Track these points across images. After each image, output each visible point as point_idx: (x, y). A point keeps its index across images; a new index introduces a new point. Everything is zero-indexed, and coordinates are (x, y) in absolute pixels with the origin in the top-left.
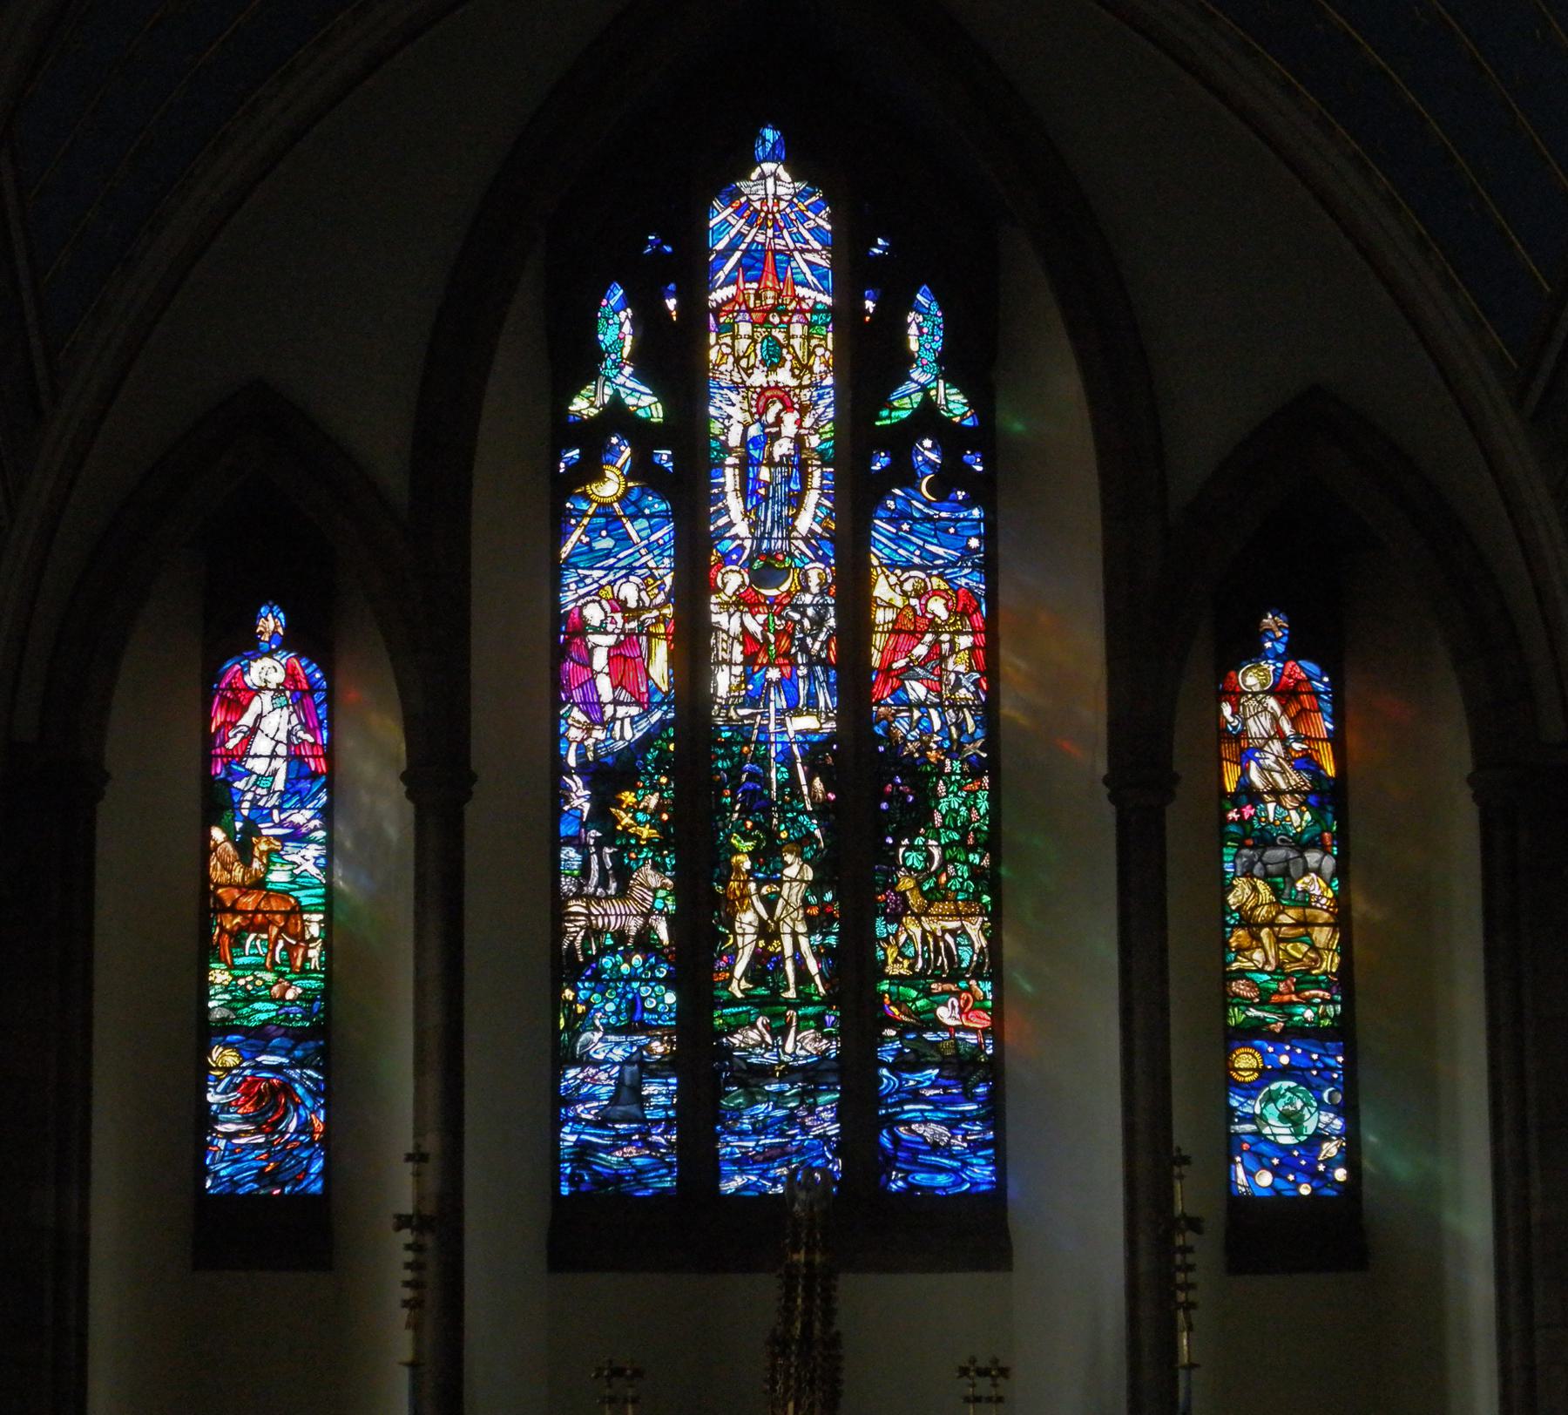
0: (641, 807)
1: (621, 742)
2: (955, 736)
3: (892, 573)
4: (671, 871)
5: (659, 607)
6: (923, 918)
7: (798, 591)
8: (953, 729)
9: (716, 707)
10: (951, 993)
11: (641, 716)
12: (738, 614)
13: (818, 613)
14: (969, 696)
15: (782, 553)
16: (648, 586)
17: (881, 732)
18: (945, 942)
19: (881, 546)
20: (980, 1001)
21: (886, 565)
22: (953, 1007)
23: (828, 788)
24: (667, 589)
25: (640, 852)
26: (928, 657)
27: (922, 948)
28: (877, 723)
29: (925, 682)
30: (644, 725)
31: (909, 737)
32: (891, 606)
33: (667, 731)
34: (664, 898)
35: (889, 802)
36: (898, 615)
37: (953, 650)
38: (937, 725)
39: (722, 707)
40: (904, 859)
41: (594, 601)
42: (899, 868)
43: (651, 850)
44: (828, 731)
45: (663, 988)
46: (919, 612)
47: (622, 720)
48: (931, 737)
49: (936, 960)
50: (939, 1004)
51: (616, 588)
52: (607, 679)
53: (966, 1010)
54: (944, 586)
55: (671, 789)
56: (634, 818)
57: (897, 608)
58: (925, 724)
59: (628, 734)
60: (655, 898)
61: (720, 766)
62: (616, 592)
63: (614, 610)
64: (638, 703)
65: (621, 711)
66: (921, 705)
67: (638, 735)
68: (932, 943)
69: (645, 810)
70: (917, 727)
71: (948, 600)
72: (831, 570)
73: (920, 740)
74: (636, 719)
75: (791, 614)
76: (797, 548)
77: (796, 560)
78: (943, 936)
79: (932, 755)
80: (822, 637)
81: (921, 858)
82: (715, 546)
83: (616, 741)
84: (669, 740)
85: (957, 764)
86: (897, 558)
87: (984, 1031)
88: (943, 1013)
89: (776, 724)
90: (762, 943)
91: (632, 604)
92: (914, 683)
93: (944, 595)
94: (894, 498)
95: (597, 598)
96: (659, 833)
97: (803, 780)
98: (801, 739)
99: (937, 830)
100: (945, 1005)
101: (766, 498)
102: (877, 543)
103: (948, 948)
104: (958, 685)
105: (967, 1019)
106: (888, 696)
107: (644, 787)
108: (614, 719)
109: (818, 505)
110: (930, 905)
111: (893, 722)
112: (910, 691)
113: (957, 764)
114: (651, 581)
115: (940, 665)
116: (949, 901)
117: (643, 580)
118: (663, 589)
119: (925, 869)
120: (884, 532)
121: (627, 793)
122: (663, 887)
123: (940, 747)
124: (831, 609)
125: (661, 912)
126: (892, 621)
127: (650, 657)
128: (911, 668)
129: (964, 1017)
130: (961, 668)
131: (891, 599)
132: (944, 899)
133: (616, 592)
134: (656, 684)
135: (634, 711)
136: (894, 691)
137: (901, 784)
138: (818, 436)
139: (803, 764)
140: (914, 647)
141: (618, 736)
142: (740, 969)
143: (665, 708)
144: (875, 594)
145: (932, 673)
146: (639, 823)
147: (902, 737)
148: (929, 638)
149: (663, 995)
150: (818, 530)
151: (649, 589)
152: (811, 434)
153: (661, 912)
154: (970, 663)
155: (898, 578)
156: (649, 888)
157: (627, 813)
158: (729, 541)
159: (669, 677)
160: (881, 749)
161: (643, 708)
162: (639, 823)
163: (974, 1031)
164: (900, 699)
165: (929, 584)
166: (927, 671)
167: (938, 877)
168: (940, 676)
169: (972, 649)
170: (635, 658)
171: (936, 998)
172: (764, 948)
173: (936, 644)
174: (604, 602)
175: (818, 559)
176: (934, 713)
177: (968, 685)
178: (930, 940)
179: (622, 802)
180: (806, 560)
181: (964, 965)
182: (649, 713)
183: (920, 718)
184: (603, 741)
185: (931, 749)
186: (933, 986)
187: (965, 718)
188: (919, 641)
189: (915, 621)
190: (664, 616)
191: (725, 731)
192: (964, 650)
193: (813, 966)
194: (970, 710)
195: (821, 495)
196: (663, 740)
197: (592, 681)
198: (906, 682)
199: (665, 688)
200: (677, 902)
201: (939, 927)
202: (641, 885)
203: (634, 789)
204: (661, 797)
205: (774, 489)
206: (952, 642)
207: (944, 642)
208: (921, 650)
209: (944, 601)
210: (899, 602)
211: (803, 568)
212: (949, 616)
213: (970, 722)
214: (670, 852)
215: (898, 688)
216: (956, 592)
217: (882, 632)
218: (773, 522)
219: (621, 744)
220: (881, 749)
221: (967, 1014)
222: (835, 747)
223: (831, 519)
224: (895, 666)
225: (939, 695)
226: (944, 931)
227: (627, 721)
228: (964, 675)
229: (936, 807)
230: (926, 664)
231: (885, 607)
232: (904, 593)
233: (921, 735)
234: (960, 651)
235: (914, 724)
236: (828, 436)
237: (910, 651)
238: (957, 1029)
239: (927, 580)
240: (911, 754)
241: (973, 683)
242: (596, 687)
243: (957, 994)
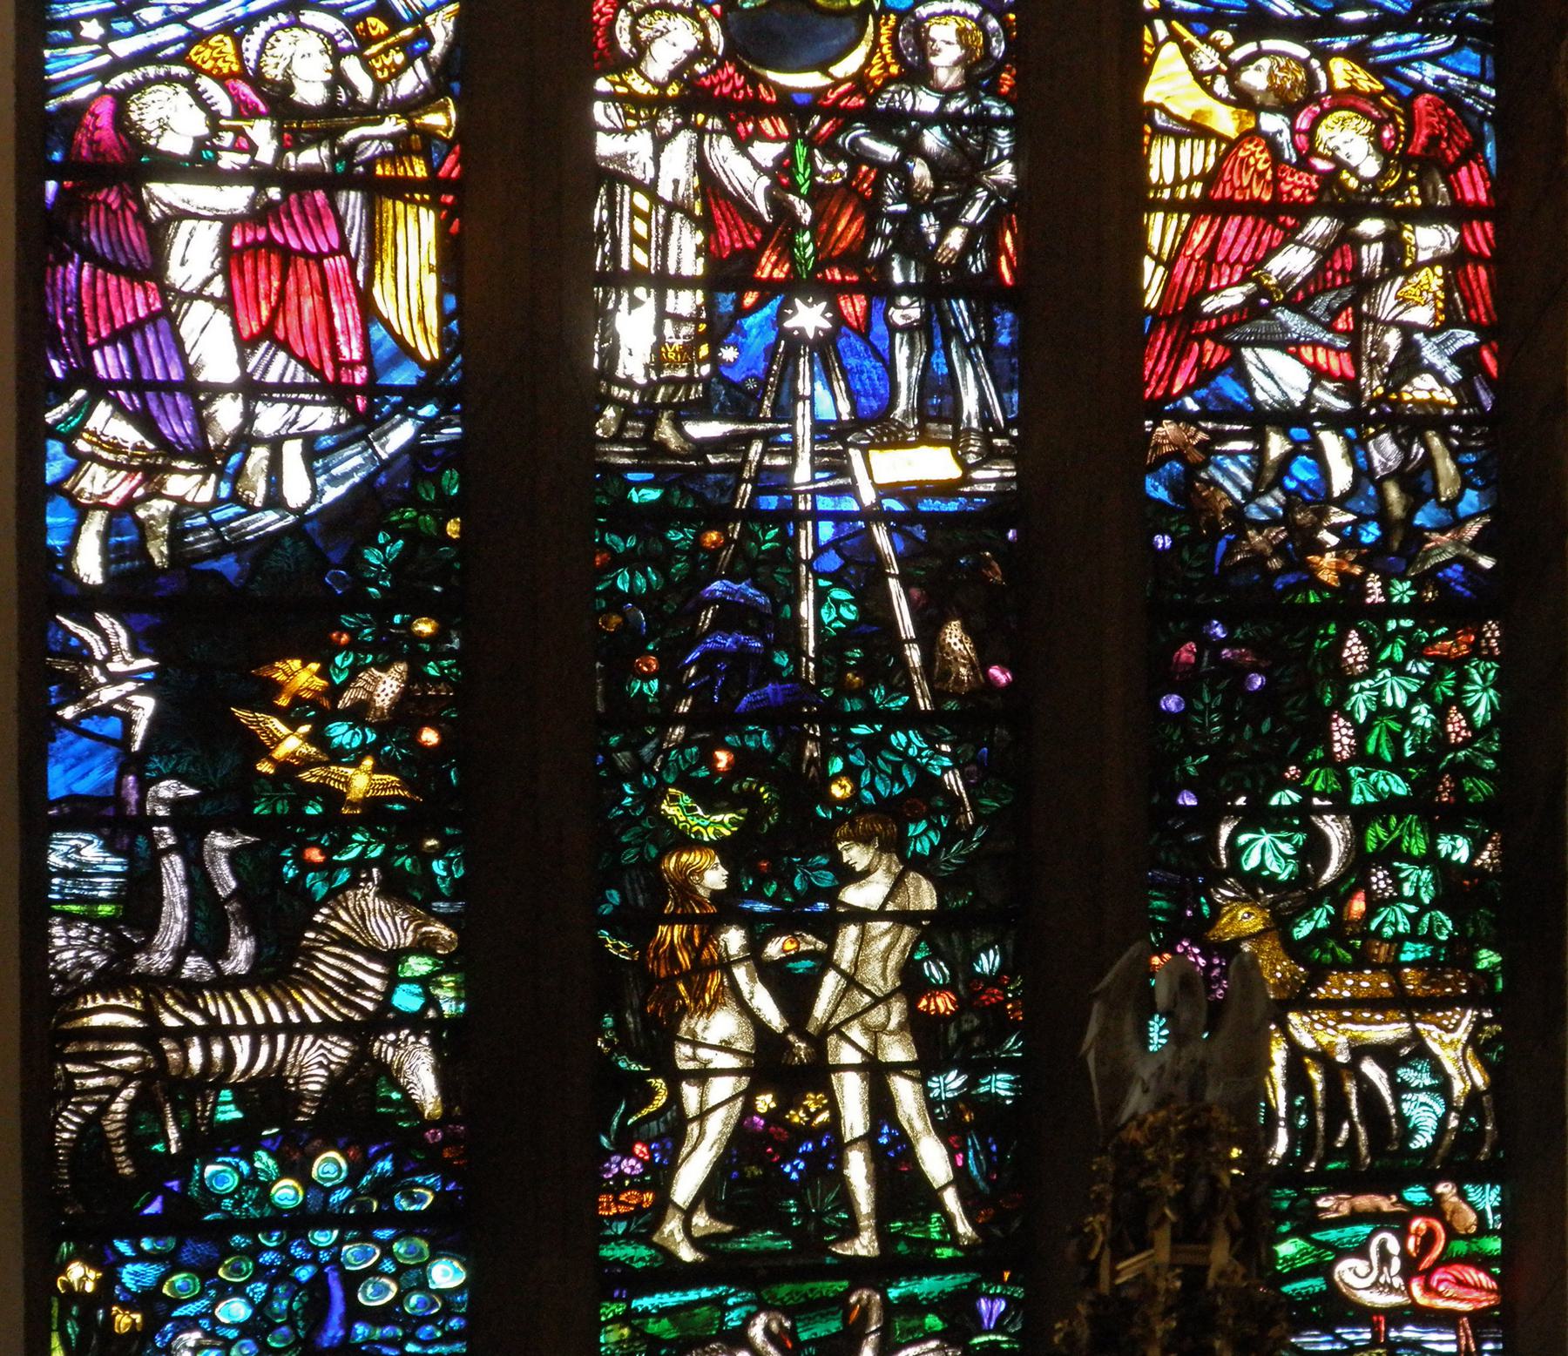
0: (346, 701)
1: (271, 516)
2: (1397, 510)
3: (1204, 39)
4: (451, 899)
5: (406, 107)
6: (1294, 1017)
8: (1393, 493)
9: (610, 413)
10: (1379, 1220)
11: (346, 436)
12: (685, 138)
14: (1445, 395)
16: (366, 40)
17: (1162, 494)
18: (1362, 1080)
20: (1467, 1237)
22: (1385, 1258)
23: (985, 652)
24: (437, 51)
25: (342, 843)
26: (1317, 282)
27: (1290, 1098)
28: (1153, 469)
29: (1307, 353)
30: (358, 460)
31: (1253, 512)
32: (1197, 130)
33: (436, 479)
34: (425, 981)
35: (1188, 693)
36: (1220, 160)
37: (1397, 261)
38: (1342, 478)
39: (628, 411)
40: (1235, 852)
41: (170, 79)
42: (1217, 878)
43: (380, 838)
44: (992, 487)
45: (423, 1245)
46: (1289, 154)
47: (275, 444)
48: (1322, 514)
49: (1332, 1130)
50: (1341, 1253)
51: (252, 45)
52: (222, 320)
53: (1426, 1264)
54: (1365, 82)
55: (450, 654)
56: (318, 738)
57: (1221, 138)
58: (1304, 476)
59: (296, 489)
60: (393, 980)
61: (623, 585)
62: (251, 55)
63: (244, 110)
64: (337, 393)
65: (270, 418)
66: (1287, 417)
67: (332, 494)
68: (1319, 1087)
69: (358, 714)
70: (1277, 483)
71: (1380, 124)
72: (1003, 22)
73: (1286, 521)
74: (326, 442)
75: (867, 142)
78: (1353, 1066)
79: (1327, 567)
80: (973, 214)
81: (1287, 849)
83: (252, 510)
84: (447, 506)
85: (1402, 591)
87: (1479, 1319)
88: (1352, 1275)
89: (815, 469)
90: (765, 1102)
91: (311, 93)
92: (1272, 357)
93: (1368, 107)
95: (183, 71)
96: (406, 783)
97: (906, 624)
98: (896, 505)
99: (1340, 769)
100: (1361, 1251)
103: (1368, 1093)
104: (1409, 363)
105: (1428, 1289)
106: (1188, 390)
107: (355, 646)
108: (244, 439)
110: (1318, 975)
111: (1204, 465)
112: (1251, 369)
113: (1402, 591)
114: (378, 26)
115: (1355, 302)
116: (1376, 968)
117: (351, 21)
118: (424, 54)
119: (1303, 879)
121: (296, 664)
122: (423, 947)
123: (1349, 541)
124: (1002, 133)
125: (415, 1022)
127: (373, 256)
128: (1265, 313)
129: (1416, 1288)
130: (1422, 315)
131: (1198, 114)
132: (1361, 961)
133: (251, 55)
134: (399, 339)
135: (320, 417)
136: (1205, 376)
137: (1228, 642)
139: (906, 582)
140: (1272, 252)
141: (258, 497)
142: (688, 1181)
143: (429, 410)
145: (1329, 327)
146: (336, 755)
147: (1227, 511)
148: (1320, 227)
149: (423, 1267)
151: (374, 49)
153: (415, 1022)
154: (1449, 300)
155: (1224, 54)
156: (373, 953)
157: (293, 725)
159: (444, 318)
160: (1162, 541)
161: (352, 408)
162: (336, 755)
163: (1446, 1319)
164: (1223, 399)
165: (1321, 76)
166: (1314, 320)
167: (1341, 903)
168: (1355, 336)
169: (1454, 262)
170: (319, 257)
171: (1332, 1235)
172: (770, 1116)
173: (1347, 240)
174: (205, 83)
176: (1332, 444)
177: (1441, 362)
178: (1316, 1075)
179: (278, 687)
181: (1421, 1141)
182: (372, 425)
183: (1287, 460)
184: (205, 509)
185: (1321, 549)
186: (1321, 1203)
187: (1429, 459)
188: (1290, 237)
189: (1276, 180)
190: (428, 134)
191: (639, 485)
192: (1431, 263)
193: (934, 1160)
194: (1445, 436)
196: (421, 506)
197: (166, 317)
198: (1247, 353)
199: (429, 349)
200: (465, 991)
201: (1342, 1040)
202: (345, 942)
203: (318, 651)
204: (415, 676)
206: (1394, 244)
207: (1370, 241)
208: (1295, 262)
209: (1367, 126)
210: (1226, 121)
212: (1385, 168)
213: (1446, 467)
214: (447, 844)
215: (1221, 368)
216: (1407, 103)
217: (1173, 206)
219: (270, 520)
220: (1162, 541)
221: (1429, 1273)
222: (1011, 534)
224: (1210, 305)
225: (1350, 389)
226: (1360, 1051)
227: (292, 451)
228: (1429, 333)
229: (1339, 705)
230: (1310, 299)
231: (1179, 137)
232: (1243, 100)
233: (1288, 507)
234: (1417, 267)
235: (1269, 475)
237: (1260, 263)
238: (1396, 1316)
239: (1315, 63)
240: (1258, 559)
241: (1455, 359)
242: (179, 342)
243: (1398, 1223)
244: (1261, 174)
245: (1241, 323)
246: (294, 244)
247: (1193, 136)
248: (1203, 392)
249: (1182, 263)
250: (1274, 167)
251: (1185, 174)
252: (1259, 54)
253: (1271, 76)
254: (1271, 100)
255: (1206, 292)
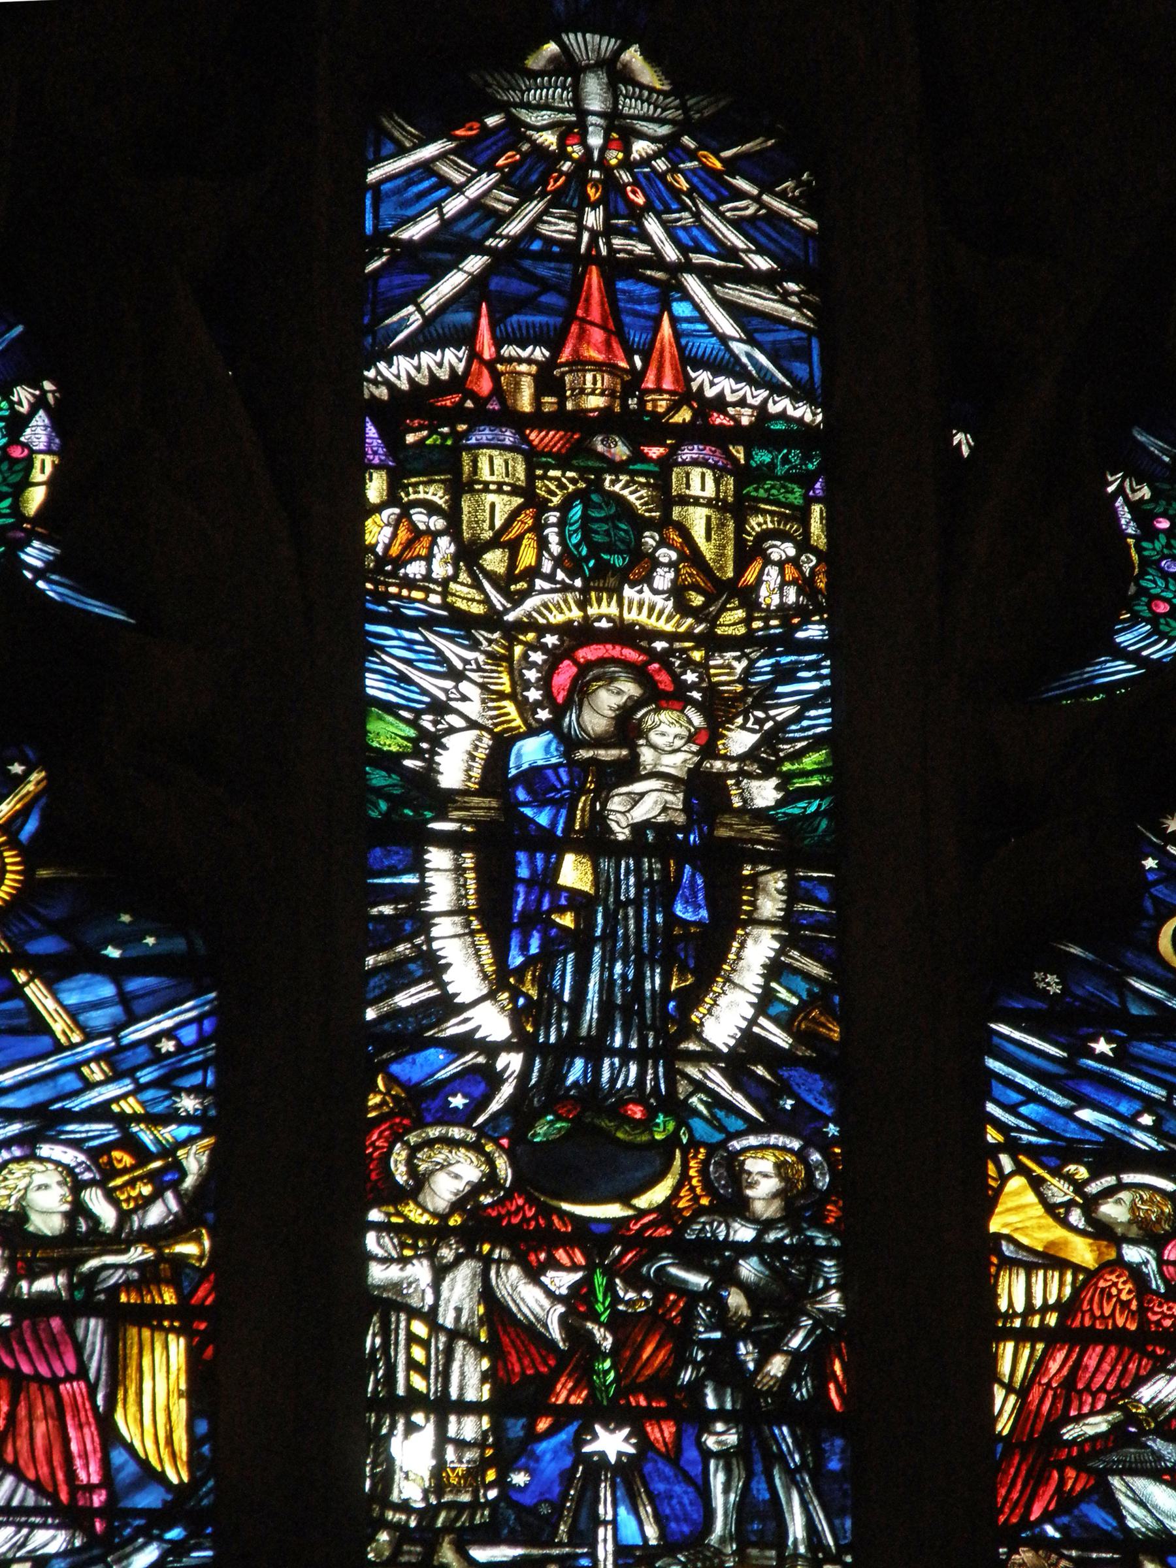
7: (700, 1211)
13: (777, 1273)
15: (641, 1100)
19: (1015, 1097)
21: (1033, 1151)
32: (1051, 1260)
39: (402, 1534)
57: (1077, 1268)
76: (699, 1087)
77: (696, 1123)
82: (383, 1067)
86: (1072, 1131)
94: (1063, 966)
101: (581, 941)
102: (998, 1089)
106: (1047, 1517)
109: (775, 970)
112: (1121, 1498)
120: (1022, 1054)
126: (1058, 1306)
127: (116, 1380)
134: (144, 1464)
136: (1066, 1503)
138: (774, 781)
140: (1140, 1381)
144: (995, 1225)
150: (780, 1038)
152: (750, 776)
158: (440, 1056)
159: (194, 1442)
170: (55, 1382)
175: (775, 1122)
180: (735, 1124)
182: (112, 1548)
195: (786, 943)
198: (1116, 1482)
199: (178, 1474)
205: (610, 918)
211: (723, 1144)
218: (606, 1007)
223: (828, 1010)
224: (1070, 1432)
232: (1101, 1231)
236: (815, 782)
244: (1125, 1305)
245: (1107, 1451)
246: (26, 1369)
247: (1046, 1268)
248: (1065, 1520)
249: (1036, 1391)
250: (1140, 1297)
251: (1038, 1302)
252: (1121, 1186)
253: (1133, 1208)
254: (1134, 1232)
255: (1067, 1420)
